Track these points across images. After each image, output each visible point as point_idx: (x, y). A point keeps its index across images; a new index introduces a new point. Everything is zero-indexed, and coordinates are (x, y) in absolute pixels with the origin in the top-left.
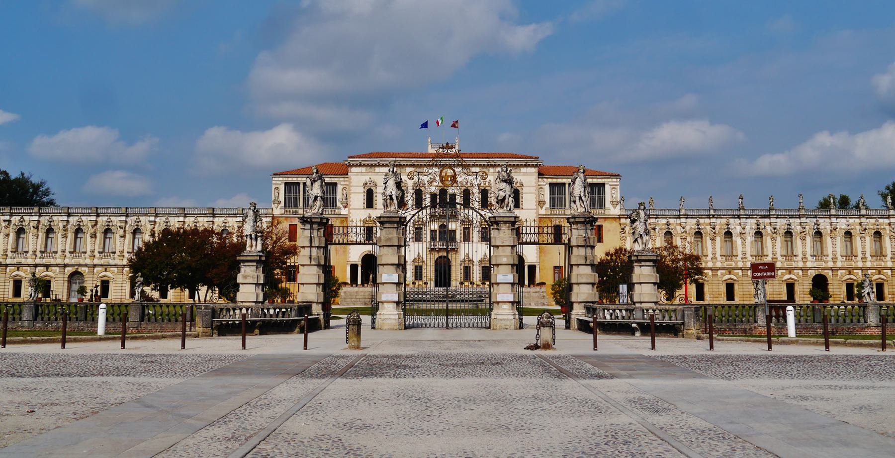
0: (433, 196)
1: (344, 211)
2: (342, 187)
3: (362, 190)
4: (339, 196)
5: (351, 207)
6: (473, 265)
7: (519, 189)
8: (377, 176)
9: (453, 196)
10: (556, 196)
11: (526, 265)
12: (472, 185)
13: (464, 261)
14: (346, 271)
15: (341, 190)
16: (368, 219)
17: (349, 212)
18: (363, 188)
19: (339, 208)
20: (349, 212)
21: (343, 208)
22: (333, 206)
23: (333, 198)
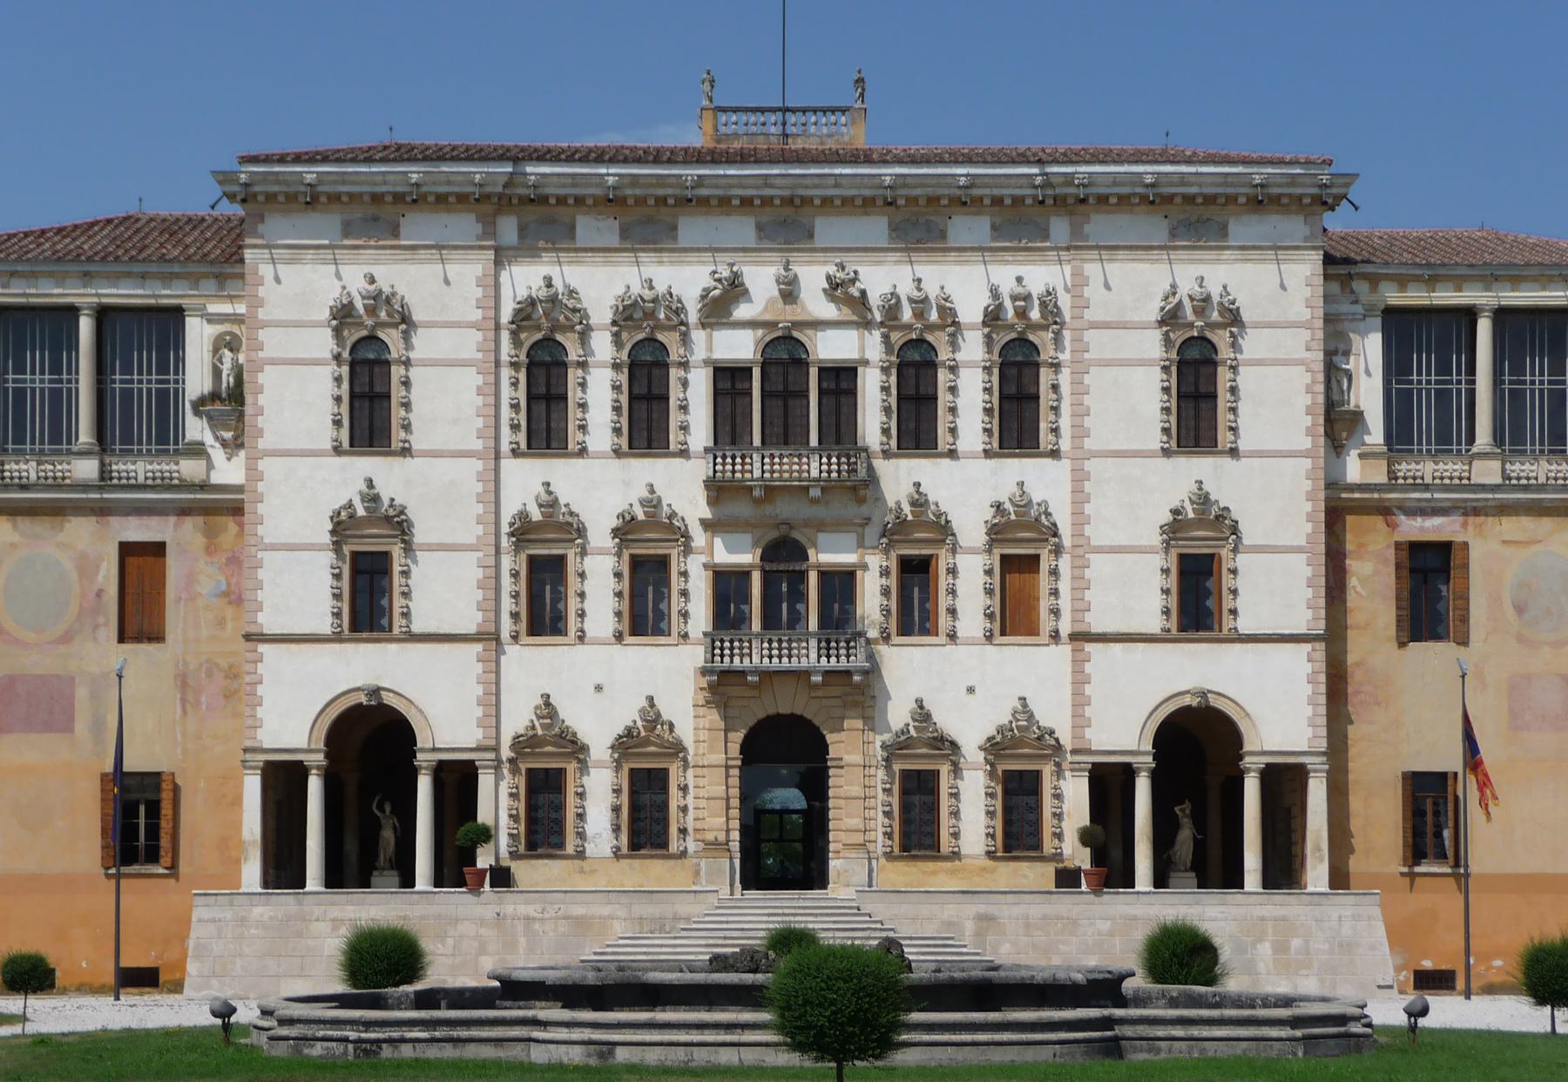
0: (728, 379)
1: (227, 470)
2: (211, 330)
3: (323, 343)
4: (197, 379)
5: (262, 444)
6: (956, 771)
7: (1221, 339)
8: (412, 269)
9: (841, 378)
10: (1424, 379)
11: (1252, 764)
12: (950, 319)
13: (898, 747)
14: (237, 801)
15: (207, 347)
16: (361, 512)
17: (251, 469)
18: (329, 332)
19: (198, 450)
20: (253, 473)
21: (217, 454)
22: (163, 439)
23: (163, 395)
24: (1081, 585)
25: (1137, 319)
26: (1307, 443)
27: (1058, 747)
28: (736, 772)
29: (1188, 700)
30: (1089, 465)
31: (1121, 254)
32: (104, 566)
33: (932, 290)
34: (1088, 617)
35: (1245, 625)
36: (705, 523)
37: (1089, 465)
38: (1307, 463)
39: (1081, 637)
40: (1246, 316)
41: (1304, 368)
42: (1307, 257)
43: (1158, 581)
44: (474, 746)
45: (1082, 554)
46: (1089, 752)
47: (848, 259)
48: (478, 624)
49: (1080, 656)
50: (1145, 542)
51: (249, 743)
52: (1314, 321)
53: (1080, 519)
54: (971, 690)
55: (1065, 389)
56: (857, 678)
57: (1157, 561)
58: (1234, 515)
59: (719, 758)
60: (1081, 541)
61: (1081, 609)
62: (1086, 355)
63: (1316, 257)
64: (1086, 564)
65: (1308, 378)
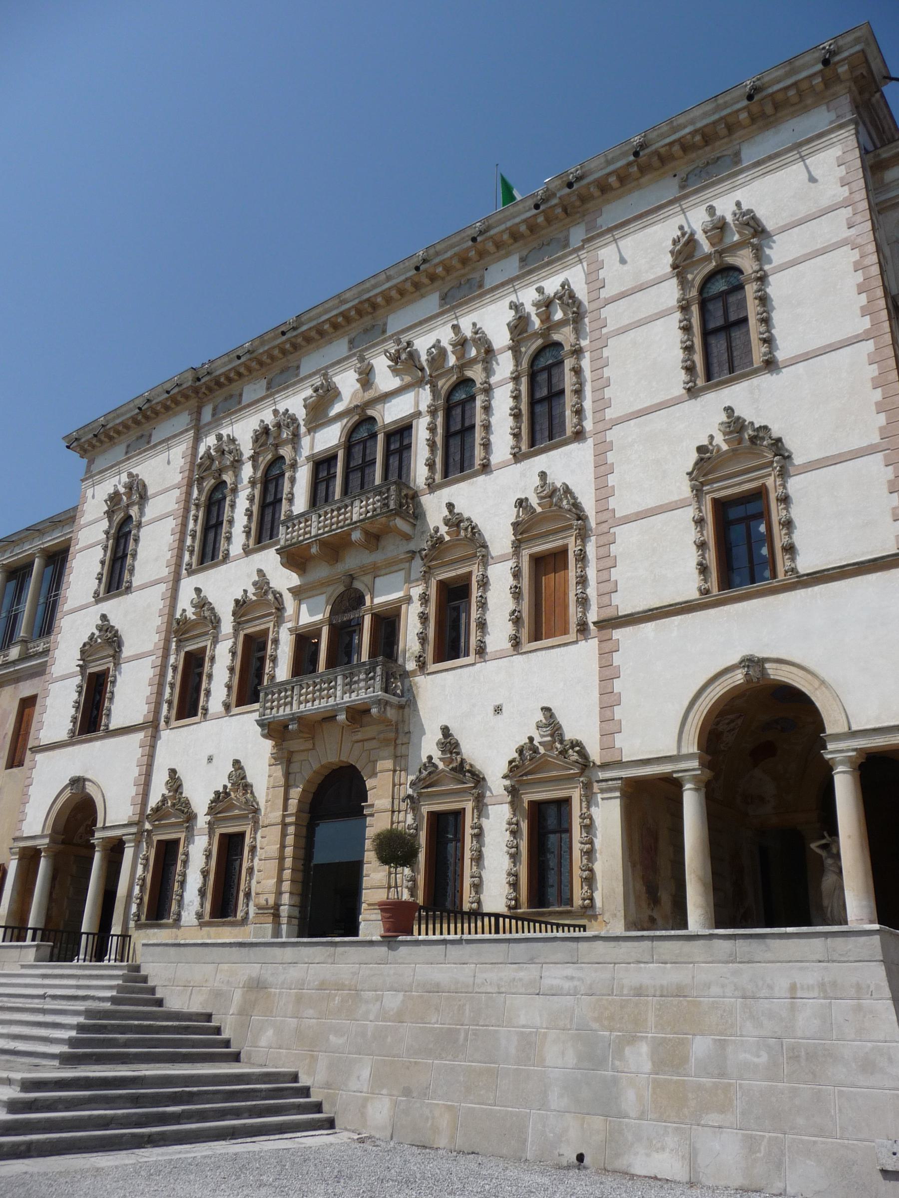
7: (744, 260)
24: (608, 562)
25: (652, 277)
26: (866, 323)
27: (585, 763)
28: (291, 830)
29: (739, 677)
30: (610, 436)
31: (633, 226)
32: (11, 716)
33: (468, 332)
34: (616, 599)
35: (806, 563)
36: (296, 592)
37: (610, 436)
38: (869, 346)
39: (605, 624)
40: (769, 225)
41: (847, 248)
42: (835, 140)
43: (691, 534)
44: (126, 822)
45: (606, 530)
46: (619, 764)
47: (412, 336)
48: (145, 715)
49: (608, 646)
50: (675, 497)
51: (18, 834)
52: (853, 195)
53: (604, 492)
54: (498, 710)
55: (587, 373)
56: (374, 711)
57: (690, 513)
58: (776, 433)
59: (276, 815)
60: (605, 516)
61: (609, 589)
62: (604, 331)
63: (846, 134)
64: (611, 539)
65: (855, 255)
